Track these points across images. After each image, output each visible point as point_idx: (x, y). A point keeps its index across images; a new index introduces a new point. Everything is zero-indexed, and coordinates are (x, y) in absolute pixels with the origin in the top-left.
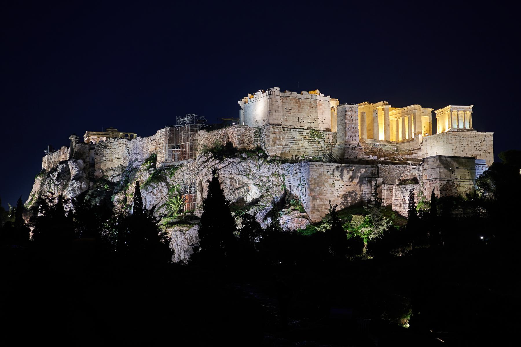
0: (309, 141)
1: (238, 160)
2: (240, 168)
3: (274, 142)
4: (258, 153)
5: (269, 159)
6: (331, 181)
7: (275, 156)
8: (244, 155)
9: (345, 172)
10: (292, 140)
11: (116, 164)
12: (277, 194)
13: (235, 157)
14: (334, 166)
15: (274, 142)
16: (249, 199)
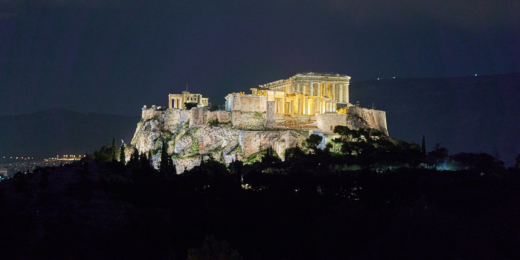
0: (254, 118)
1: (218, 128)
2: (219, 131)
3: (236, 119)
4: (228, 124)
5: (233, 127)
6: (254, 139)
7: (236, 126)
8: (221, 126)
9: (262, 135)
10: (245, 118)
12: (234, 144)
13: (217, 126)
14: (256, 132)
15: (236, 119)
16: (223, 146)
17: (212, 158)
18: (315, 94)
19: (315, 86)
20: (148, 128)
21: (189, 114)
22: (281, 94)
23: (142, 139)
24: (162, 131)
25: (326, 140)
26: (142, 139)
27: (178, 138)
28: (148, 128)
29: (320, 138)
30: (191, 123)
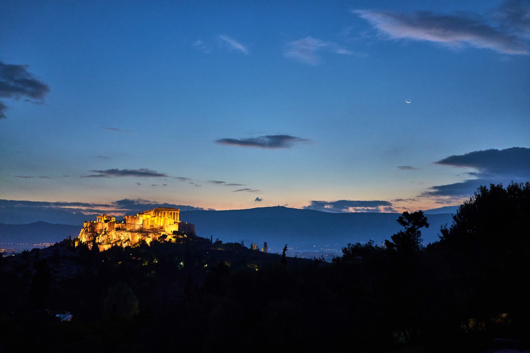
4: (124, 230)
11: (99, 229)
12: (127, 239)
17: (116, 245)
18: (164, 216)
19: (164, 213)
20: (86, 231)
21: (106, 225)
22: (149, 216)
23: (84, 236)
24: (94, 232)
25: (169, 237)
26: (84, 236)
27: (101, 235)
28: (87, 231)
29: (167, 236)
30: (107, 229)
